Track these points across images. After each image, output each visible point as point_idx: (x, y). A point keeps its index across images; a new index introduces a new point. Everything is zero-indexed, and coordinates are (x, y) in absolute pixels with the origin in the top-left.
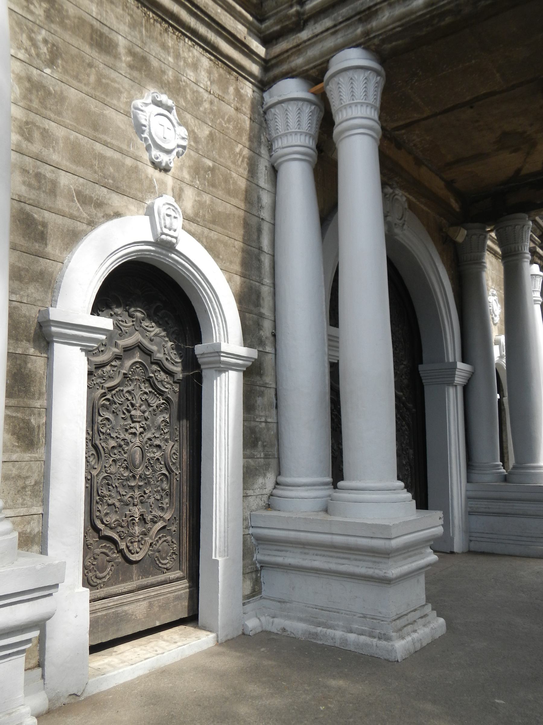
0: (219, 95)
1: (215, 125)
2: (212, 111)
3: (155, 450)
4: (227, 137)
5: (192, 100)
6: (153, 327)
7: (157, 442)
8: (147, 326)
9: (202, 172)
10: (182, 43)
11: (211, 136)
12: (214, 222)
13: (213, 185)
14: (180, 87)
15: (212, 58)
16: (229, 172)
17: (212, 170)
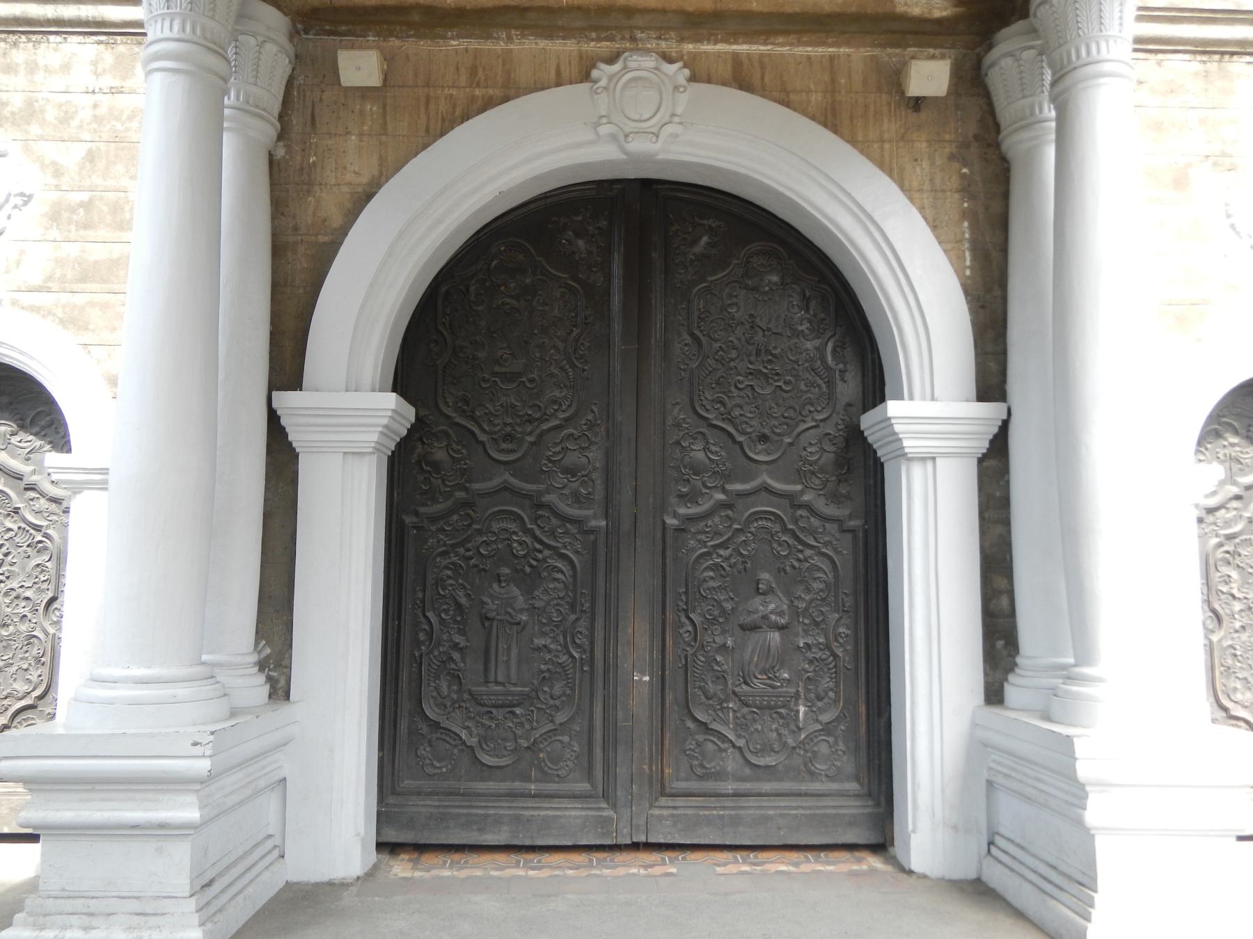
0: (111, 88)
1: (100, 137)
2: (95, 116)
3: (23, 604)
4: (124, 144)
5: (56, 118)
6: (30, 441)
7: (29, 593)
8: (20, 442)
9: (65, 215)
10: (43, 46)
11: (91, 157)
12: (83, 279)
13: (87, 226)
14: (34, 111)
15: (103, 38)
16: (123, 194)
17: (87, 205)
